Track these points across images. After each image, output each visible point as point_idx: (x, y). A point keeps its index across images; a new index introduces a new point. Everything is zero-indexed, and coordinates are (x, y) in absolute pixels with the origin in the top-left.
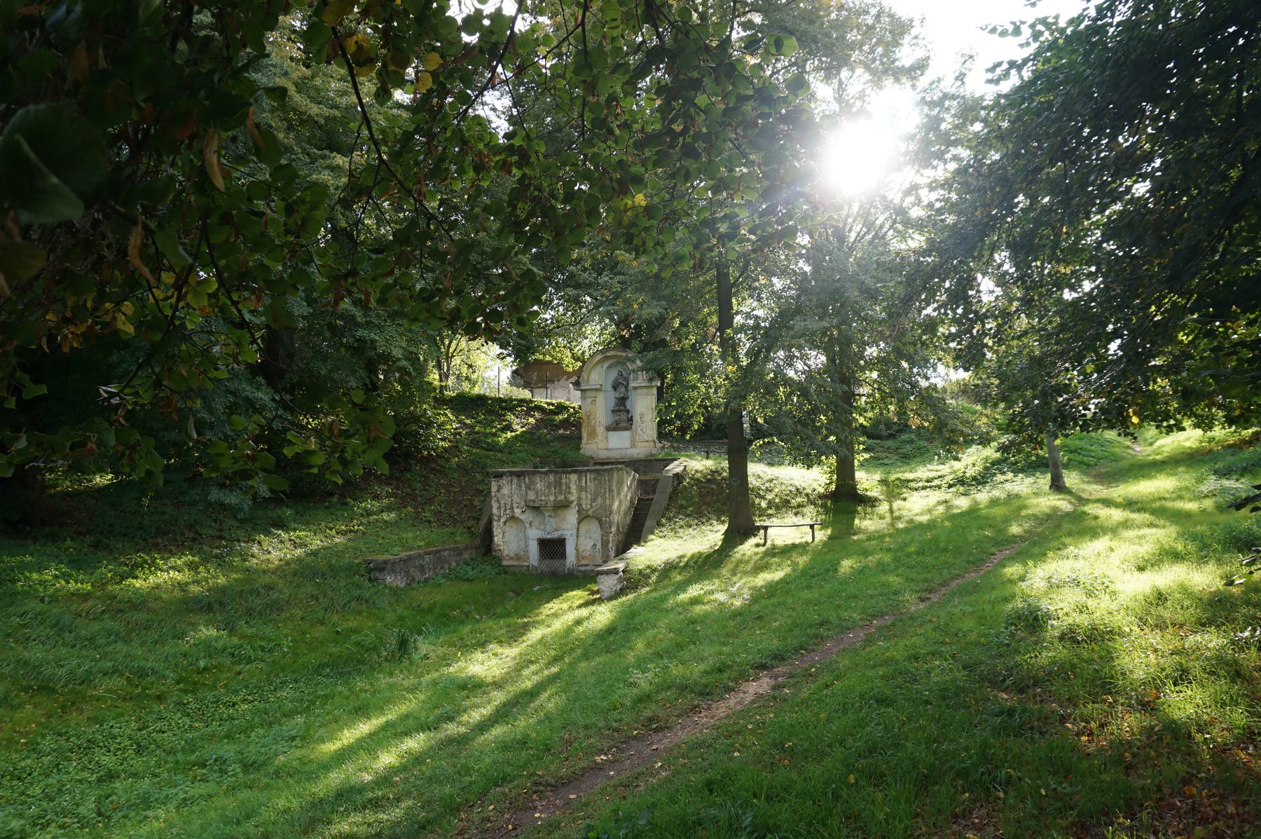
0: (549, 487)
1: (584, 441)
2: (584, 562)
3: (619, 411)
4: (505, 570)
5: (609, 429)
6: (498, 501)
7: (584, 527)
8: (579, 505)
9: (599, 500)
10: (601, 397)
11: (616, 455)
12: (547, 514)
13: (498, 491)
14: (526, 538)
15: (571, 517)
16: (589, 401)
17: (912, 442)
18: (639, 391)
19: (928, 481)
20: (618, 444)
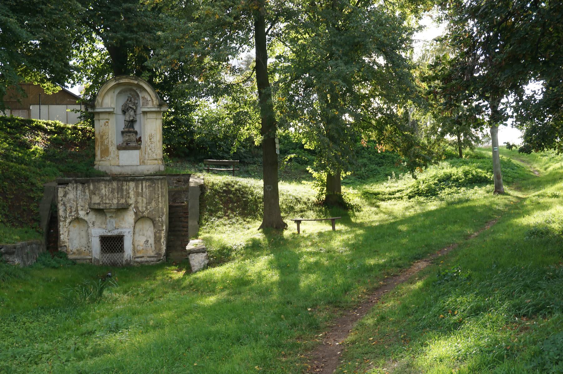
0: (112, 192)
1: (98, 157)
2: (138, 255)
3: (130, 132)
4: (74, 262)
5: (120, 148)
6: (64, 204)
7: (139, 226)
8: (136, 207)
9: (153, 203)
10: (112, 120)
11: (128, 171)
12: (108, 215)
13: (65, 196)
14: (88, 235)
15: (130, 217)
16: (102, 122)
17: (365, 165)
18: (149, 116)
19: (390, 194)
20: (128, 160)
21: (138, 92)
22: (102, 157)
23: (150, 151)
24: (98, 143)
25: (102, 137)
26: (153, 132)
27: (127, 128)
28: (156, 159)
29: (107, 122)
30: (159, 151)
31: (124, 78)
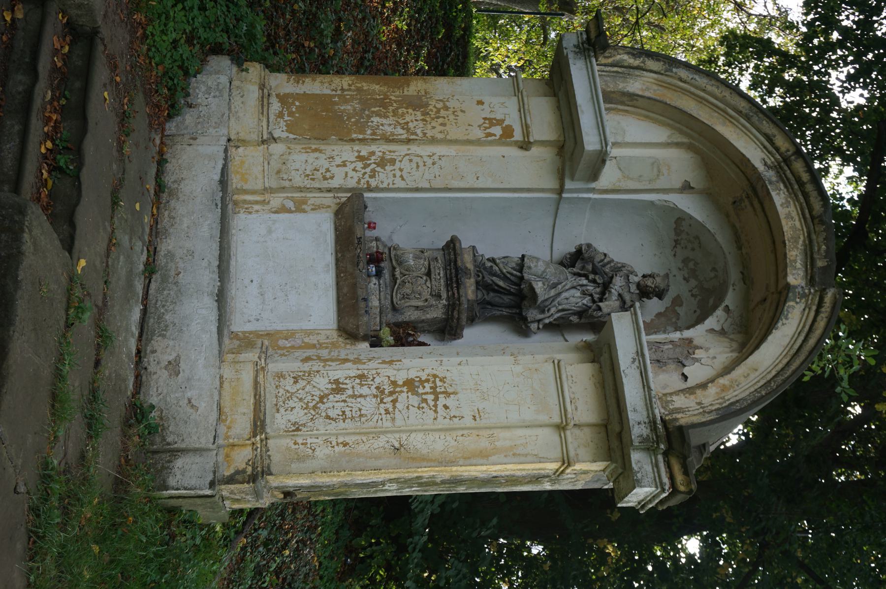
1: (281, 83)
10: (528, 170)
16: (507, 110)
18: (580, 376)
21: (711, 322)
22: (284, 99)
23: (322, 383)
24: (374, 87)
25: (418, 104)
26: (463, 404)
28: (259, 425)
29: (508, 132)
30: (322, 452)
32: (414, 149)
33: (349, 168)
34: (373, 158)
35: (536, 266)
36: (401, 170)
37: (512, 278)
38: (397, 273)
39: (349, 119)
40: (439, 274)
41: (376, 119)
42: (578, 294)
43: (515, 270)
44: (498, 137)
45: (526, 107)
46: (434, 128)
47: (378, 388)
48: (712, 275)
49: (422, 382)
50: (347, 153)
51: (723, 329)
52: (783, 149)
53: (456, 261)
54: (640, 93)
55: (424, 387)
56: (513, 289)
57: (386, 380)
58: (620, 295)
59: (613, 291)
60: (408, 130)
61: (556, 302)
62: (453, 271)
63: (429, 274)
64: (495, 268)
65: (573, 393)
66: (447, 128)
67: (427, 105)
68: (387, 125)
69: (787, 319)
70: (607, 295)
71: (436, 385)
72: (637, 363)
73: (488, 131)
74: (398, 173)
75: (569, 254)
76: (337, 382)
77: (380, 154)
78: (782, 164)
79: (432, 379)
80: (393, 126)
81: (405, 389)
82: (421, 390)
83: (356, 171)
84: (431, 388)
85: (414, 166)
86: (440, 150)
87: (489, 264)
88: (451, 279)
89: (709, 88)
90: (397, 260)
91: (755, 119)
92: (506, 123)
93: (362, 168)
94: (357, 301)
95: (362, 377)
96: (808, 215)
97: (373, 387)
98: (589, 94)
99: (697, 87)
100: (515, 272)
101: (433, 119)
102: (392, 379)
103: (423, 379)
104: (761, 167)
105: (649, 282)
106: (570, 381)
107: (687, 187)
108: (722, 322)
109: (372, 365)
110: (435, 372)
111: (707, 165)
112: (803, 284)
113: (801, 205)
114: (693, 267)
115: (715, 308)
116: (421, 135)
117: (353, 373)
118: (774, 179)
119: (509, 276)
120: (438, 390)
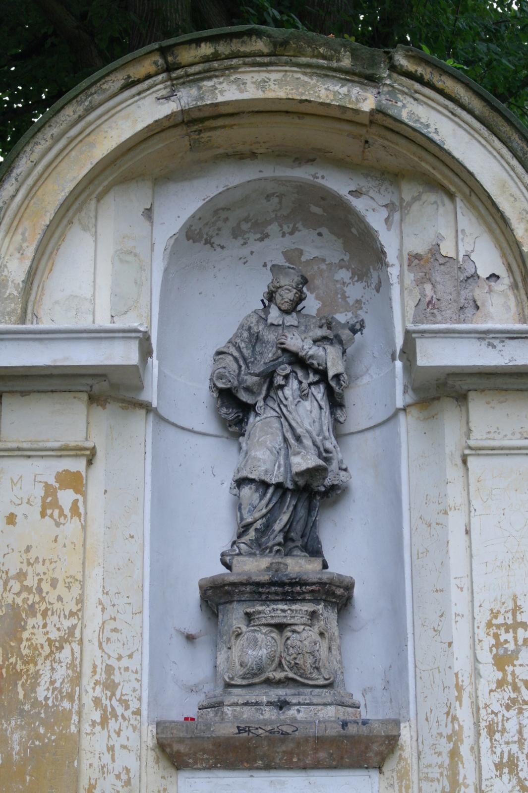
3: (288, 590)
10: (128, 454)
21: (375, 220)
27: (259, 547)
29: (75, 482)
31: (255, 61)
32: (91, 632)
33: (117, 742)
34: (105, 702)
35: (264, 463)
36: (120, 658)
37: (274, 500)
38: (279, 675)
39: (38, 737)
40: (284, 611)
41: (41, 693)
42: (307, 404)
43: (264, 494)
44: (79, 497)
45: (25, 445)
46: (60, 599)
47: (508, 708)
48: (275, 200)
49: (498, 645)
50: (93, 743)
51: (386, 206)
52: (152, 69)
53: (258, 584)
54: (28, 263)
55: (506, 642)
56: (290, 502)
57: (496, 695)
58: (315, 341)
59: (311, 353)
60: (63, 641)
61: (318, 439)
62: (273, 589)
63: (280, 627)
64: (258, 525)
65: (513, 434)
66: (60, 576)
67: (14, 607)
68: (49, 678)
69: (428, 126)
70: (315, 362)
71: (502, 625)
72: (496, 342)
73: (67, 512)
74: (125, 662)
75: (217, 410)
76: (499, 766)
77: (99, 689)
78: (174, 75)
79: (494, 630)
80: (55, 665)
81: (509, 669)
82: (511, 646)
83: (120, 730)
84: (507, 631)
85: (114, 636)
86: (94, 592)
87: (252, 534)
88: (285, 594)
89: (35, 157)
90: (255, 675)
91: (97, 98)
92: (52, 481)
93: (116, 720)
94: (346, 737)
95: (491, 730)
96: (266, 60)
97: (507, 715)
98: (31, 343)
99: (29, 175)
100: (268, 495)
101: (43, 599)
102: (494, 686)
103: (493, 642)
104: (169, 108)
105: (290, 296)
106: (496, 435)
107: (148, 213)
108: (375, 205)
109: (464, 714)
110: (483, 625)
111: (127, 180)
112: (375, 91)
113: (245, 64)
114: (250, 224)
115: (349, 210)
116: (74, 621)
117: (485, 742)
118: (194, 91)
119: (271, 505)
120: (510, 622)
